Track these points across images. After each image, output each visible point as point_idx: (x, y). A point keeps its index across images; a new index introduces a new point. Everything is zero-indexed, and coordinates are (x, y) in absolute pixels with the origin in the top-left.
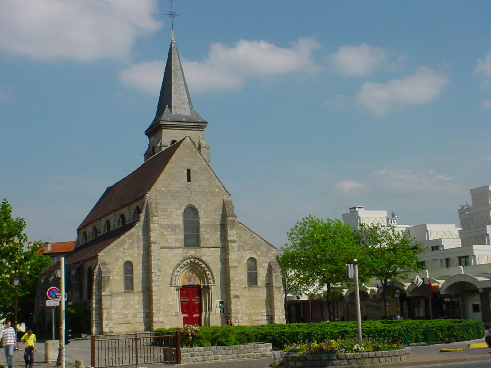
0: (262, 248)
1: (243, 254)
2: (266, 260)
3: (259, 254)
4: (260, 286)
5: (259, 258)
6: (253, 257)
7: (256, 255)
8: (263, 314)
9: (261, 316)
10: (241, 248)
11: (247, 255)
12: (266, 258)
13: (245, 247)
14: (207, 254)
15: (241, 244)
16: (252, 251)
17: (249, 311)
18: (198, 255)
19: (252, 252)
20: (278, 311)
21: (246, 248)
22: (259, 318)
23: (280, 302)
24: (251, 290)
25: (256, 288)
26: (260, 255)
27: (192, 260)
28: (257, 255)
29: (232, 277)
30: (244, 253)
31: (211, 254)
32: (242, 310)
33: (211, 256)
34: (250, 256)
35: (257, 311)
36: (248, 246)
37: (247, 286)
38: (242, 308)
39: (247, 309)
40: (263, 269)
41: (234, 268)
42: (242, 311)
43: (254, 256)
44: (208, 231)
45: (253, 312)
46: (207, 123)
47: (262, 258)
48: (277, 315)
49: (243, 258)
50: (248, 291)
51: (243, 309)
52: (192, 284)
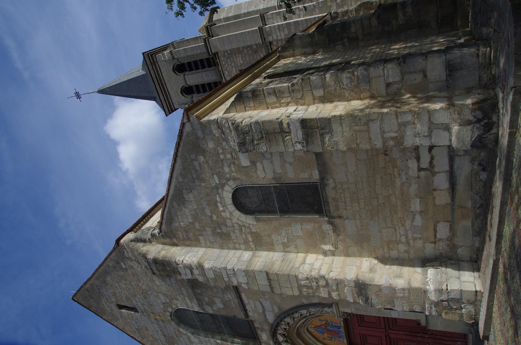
0: (198, 168)
1: (233, 226)
2: (229, 156)
3: (215, 176)
4: (316, 176)
5: (228, 180)
6: (230, 196)
7: (223, 190)
8: (425, 164)
9: (434, 174)
10: (219, 231)
11: (231, 213)
12: (222, 157)
13: (212, 220)
14: (261, 311)
15: (209, 231)
16: (216, 202)
17: (413, 220)
18: (267, 327)
19: (218, 199)
20: (409, 132)
21: (215, 218)
22: (441, 181)
23: (367, 124)
24: (337, 208)
25: (330, 193)
26: (221, 175)
27: (281, 339)
28: (223, 186)
29: (300, 291)
30: (229, 223)
31: (258, 303)
32: (411, 242)
33: (261, 303)
34: (232, 208)
35: (413, 189)
36: (208, 212)
37: (326, 219)
38: (403, 239)
39: (408, 223)
40: (259, 165)
41: (272, 282)
42: (415, 239)
43: (227, 195)
44: (207, 299)
45: (416, 205)
46: (143, 54)
47: (226, 170)
48: (430, 136)
49: (244, 226)
50: (340, 217)
51: (407, 237)
52: (342, 330)
